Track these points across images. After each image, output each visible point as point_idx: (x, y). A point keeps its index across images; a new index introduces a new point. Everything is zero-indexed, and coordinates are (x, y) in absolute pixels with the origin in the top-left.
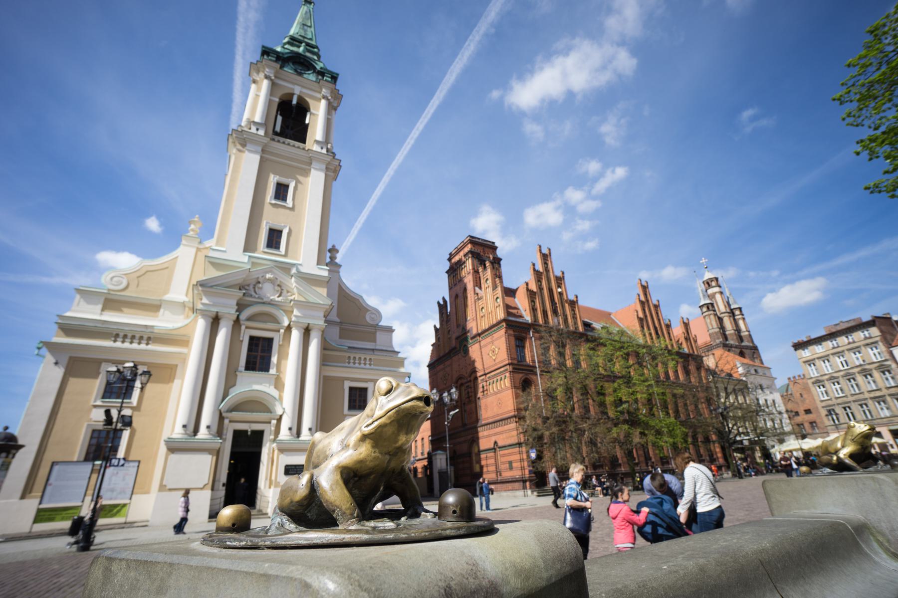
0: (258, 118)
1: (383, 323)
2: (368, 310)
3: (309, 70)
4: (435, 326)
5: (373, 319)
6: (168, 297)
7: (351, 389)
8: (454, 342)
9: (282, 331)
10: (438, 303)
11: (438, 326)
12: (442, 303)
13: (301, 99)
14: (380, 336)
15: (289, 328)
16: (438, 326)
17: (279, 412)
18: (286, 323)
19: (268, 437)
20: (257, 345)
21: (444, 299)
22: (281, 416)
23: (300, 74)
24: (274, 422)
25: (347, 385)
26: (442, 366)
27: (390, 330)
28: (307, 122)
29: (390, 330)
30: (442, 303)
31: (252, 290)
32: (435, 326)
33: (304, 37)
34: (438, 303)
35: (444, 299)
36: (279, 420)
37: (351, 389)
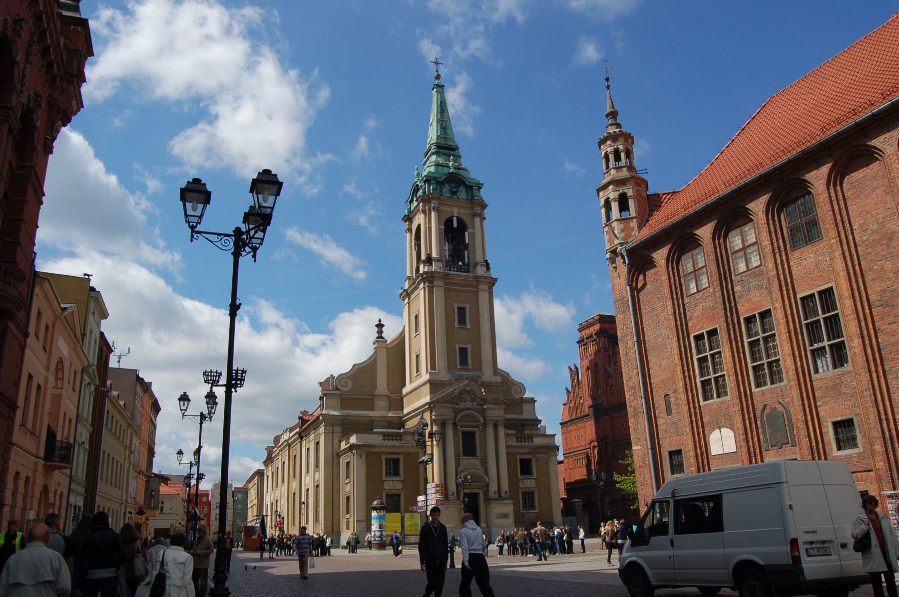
1: (527, 395)
2: (514, 384)
3: (460, 186)
6: (377, 392)
8: (586, 409)
10: (570, 368)
11: (570, 390)
12: (573, 368)
13: (460, 220)
14: (526, 407)
15: (484, 425)
19: (481, 497)
25: (518, 457)
26: (574, 427)
27: (532, 401)
28: (467, 242)
29: (532, 401)
30: (573, 368)
34: (570, 368)
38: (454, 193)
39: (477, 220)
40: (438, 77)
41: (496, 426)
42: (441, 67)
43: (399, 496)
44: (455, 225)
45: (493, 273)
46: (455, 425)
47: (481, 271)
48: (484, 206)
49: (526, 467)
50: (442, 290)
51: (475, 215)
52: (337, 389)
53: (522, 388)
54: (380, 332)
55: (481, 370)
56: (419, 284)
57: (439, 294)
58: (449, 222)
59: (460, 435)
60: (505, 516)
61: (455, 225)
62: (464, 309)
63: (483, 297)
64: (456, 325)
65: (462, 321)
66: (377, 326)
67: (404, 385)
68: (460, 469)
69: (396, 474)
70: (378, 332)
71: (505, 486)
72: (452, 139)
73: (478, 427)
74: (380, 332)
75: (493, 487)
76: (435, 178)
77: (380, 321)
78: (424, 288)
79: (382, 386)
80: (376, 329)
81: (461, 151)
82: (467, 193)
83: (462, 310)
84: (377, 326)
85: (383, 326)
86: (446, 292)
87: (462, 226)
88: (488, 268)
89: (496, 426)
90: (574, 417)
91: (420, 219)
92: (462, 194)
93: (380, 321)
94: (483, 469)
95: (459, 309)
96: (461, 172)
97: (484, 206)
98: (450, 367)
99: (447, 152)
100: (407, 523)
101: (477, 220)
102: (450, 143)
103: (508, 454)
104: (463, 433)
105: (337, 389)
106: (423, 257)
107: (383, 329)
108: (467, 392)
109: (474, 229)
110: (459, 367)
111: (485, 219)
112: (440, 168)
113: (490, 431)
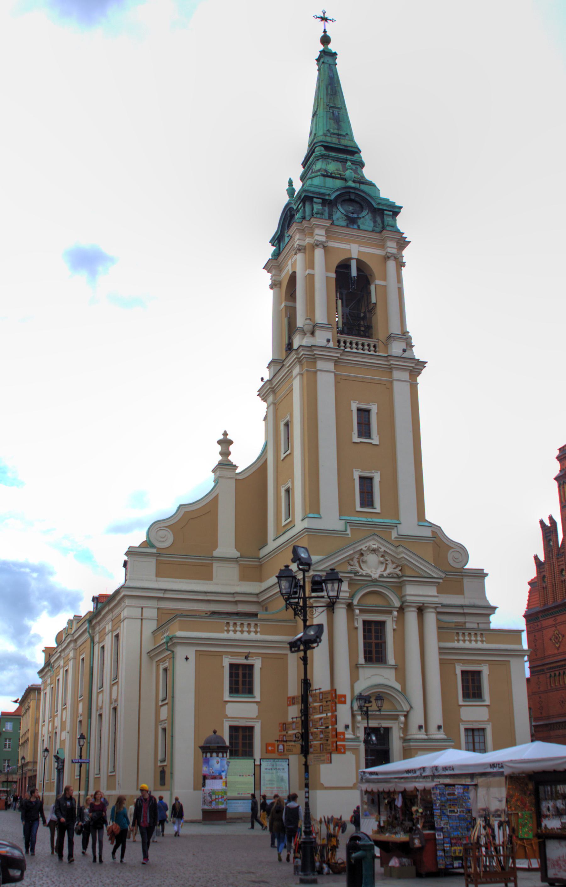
0: (320, 317)
3: (362, 209)
4: (536, 558)
5: (455, 559)
6: (216, 553)
7: (463, 672)
9: (395, 613)
10: (542, 522)
11: (542, 558)
12: (548, 523)
15: (401, 610)
16: (542, 558)
17: (406, 707)
18: (397, 604)
20: (370, 631)
21: (551, 518)
22: (408, 712)
23: (352, 221)
24: (402, 719)
26: (550, 622)
28: (373, 300)
29: (480, 575)
30: (548, 523)
31: (357, 564)
32: (536, 558)
33: (338, 135)
34: (542, 522)
35: (551, 518)
36: (406, 716)
37: (463, 672)
39: (391, 264)
40: (325, 40)
41: (421, 610)
43: (251, 729)
44: (354, 273)
45: (418, 353)
46: (350, 606)
47: (396, 348)
48: (403, 243)
49: (472, 686)
50: (331, 378)
51: (387, 258)
52: (153, 546)
53: (462, 552)
54: (225, 453)
55: (396, 515)
56: (292, 367)
57: (326, 382)
58: (343, 269)
59: (360, 625)
61: (354, 273)
62: (368, 411)
63: (400, 390)
64: (356, 439)
65: (365, 429)
66: (219, 442)
67: (264, 543)
69: (250, 691)
70: (221, 454)
72: (349, 135)
73: (390, 612)
74: (225, 453)
75: (417, 718)
76: (321, 196)
77: (225, 434)
78: (301, 375)
79: (226, 546)
80: (219, 448)
81: (364, 156)
82: (375, 222)
83: (364, 413)
84: (219, 442)
85: (231, 442)
86: (337, 382)
87: (365, 278)
88: (410, 346)
89: (421, 610)
90: (550, 604)
91: (296, 263)
92: (366, 221)
93: (225, 434)
94: (398, 686)
95: (359, 410)
96: (363, 187)
97: (403, 243)
98: (344, 507)
99: (341, 156)
100: (266, 777)
101: (391, 264)
102: (344, 142)
103: (442, 662)
104: (365, 622)
105: (153, 546)
106: (300, 322)
107: (232, 448)
108: (374, 551)
109: (385, 279)
110: (358, 509)
111: (403, 264)
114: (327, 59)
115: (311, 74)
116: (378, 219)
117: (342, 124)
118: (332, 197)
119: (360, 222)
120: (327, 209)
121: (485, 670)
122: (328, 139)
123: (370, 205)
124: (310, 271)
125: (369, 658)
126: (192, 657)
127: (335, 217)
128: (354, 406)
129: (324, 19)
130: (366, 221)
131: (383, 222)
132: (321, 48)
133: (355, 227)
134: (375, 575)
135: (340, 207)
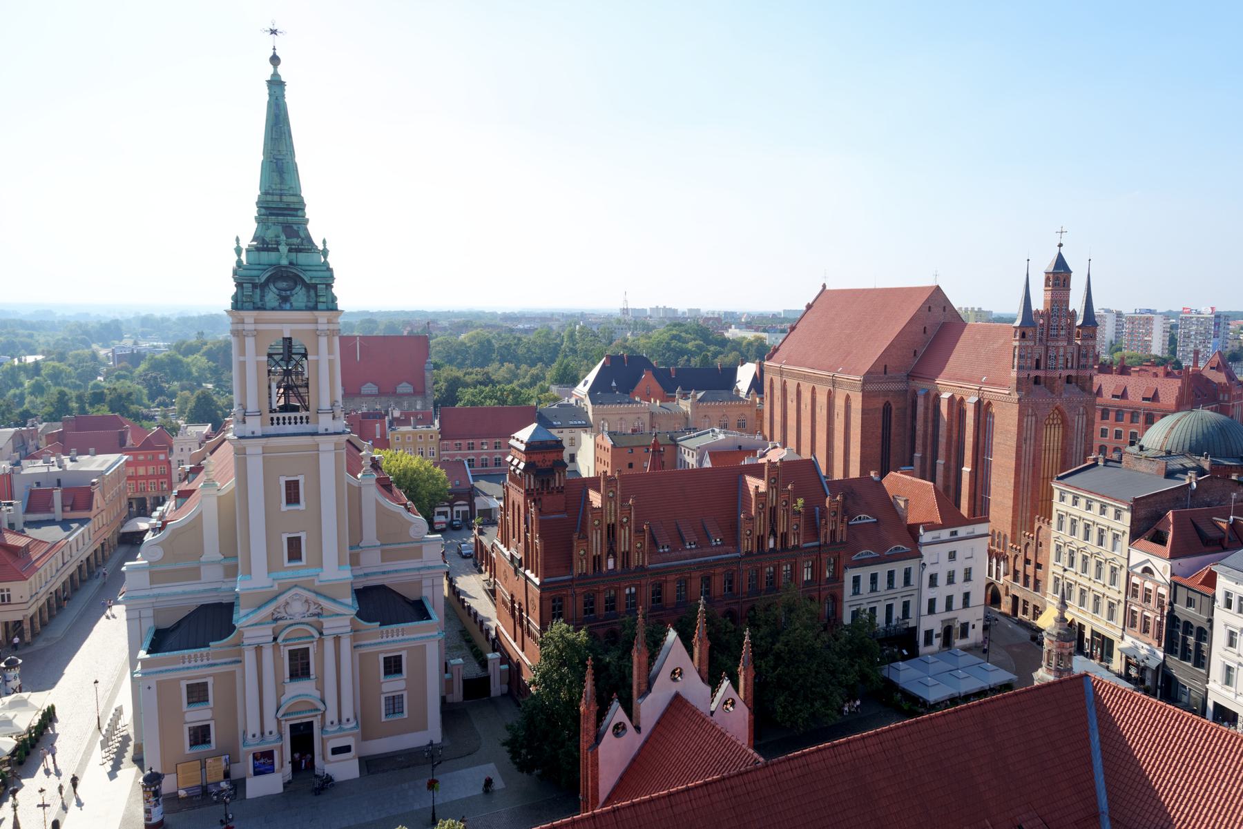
3: (296, 284)
23: (285, 299)
38: (285, 299)
40: (275, 60)
42: (278, 39)
60: (347, 749)
64: (284, 507)
68: (283, 699)
71: (348, 712)
75: (331, 715)
82: (308, 296)
89: (337, 639)
92: (300, 296)
94: (317, 694)
112: (264, 254)
113: (329, 645)
114: (276, 85)
115: (264, 95)
116: (312, 293)
117: (286, 176)
118: (263, 280)
119: (292, 299)
120: (258, 291)
121: (404, 654)
122: (269, 198)
123: (303, 280)
124: (242, 359)
125: (294, 676)
126: (154, 686)
127: (266, 299)
128: (283, 480)
129: (274, 32)
130: (300, 296)
131: (317, 296)
132: (271, 69)
133: (288, 306)
134: (298, 619)
135: (272, 286)
